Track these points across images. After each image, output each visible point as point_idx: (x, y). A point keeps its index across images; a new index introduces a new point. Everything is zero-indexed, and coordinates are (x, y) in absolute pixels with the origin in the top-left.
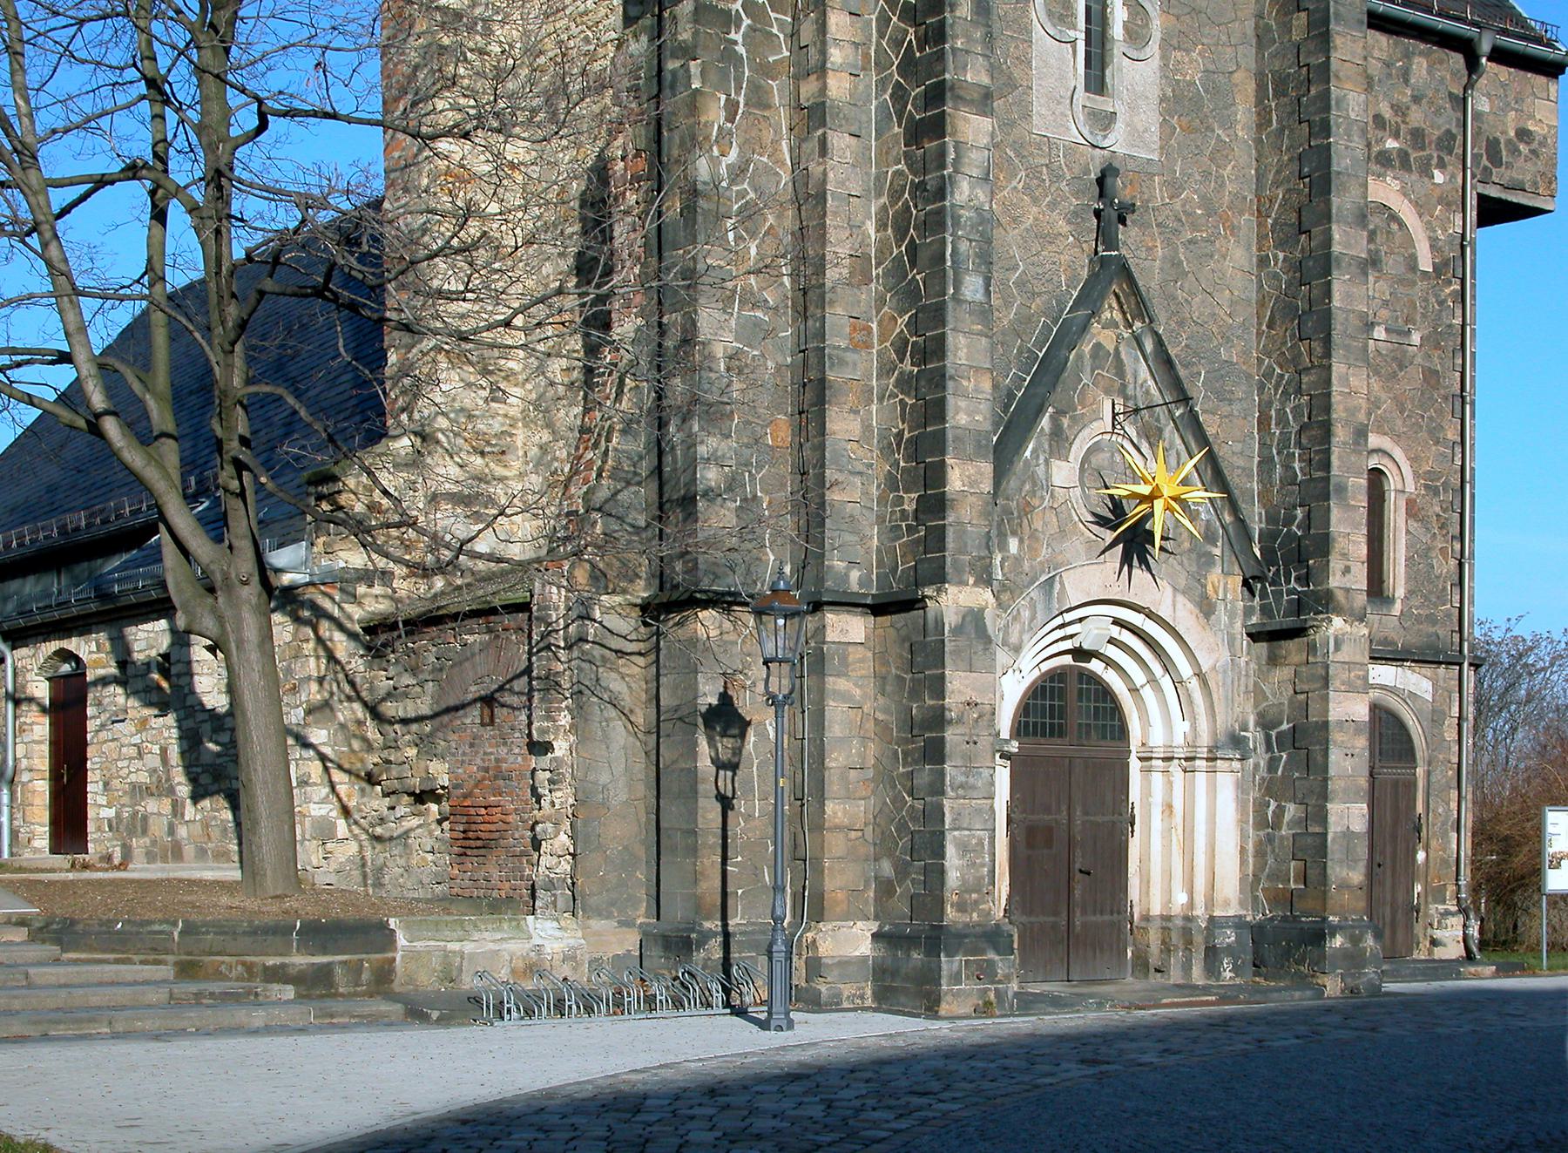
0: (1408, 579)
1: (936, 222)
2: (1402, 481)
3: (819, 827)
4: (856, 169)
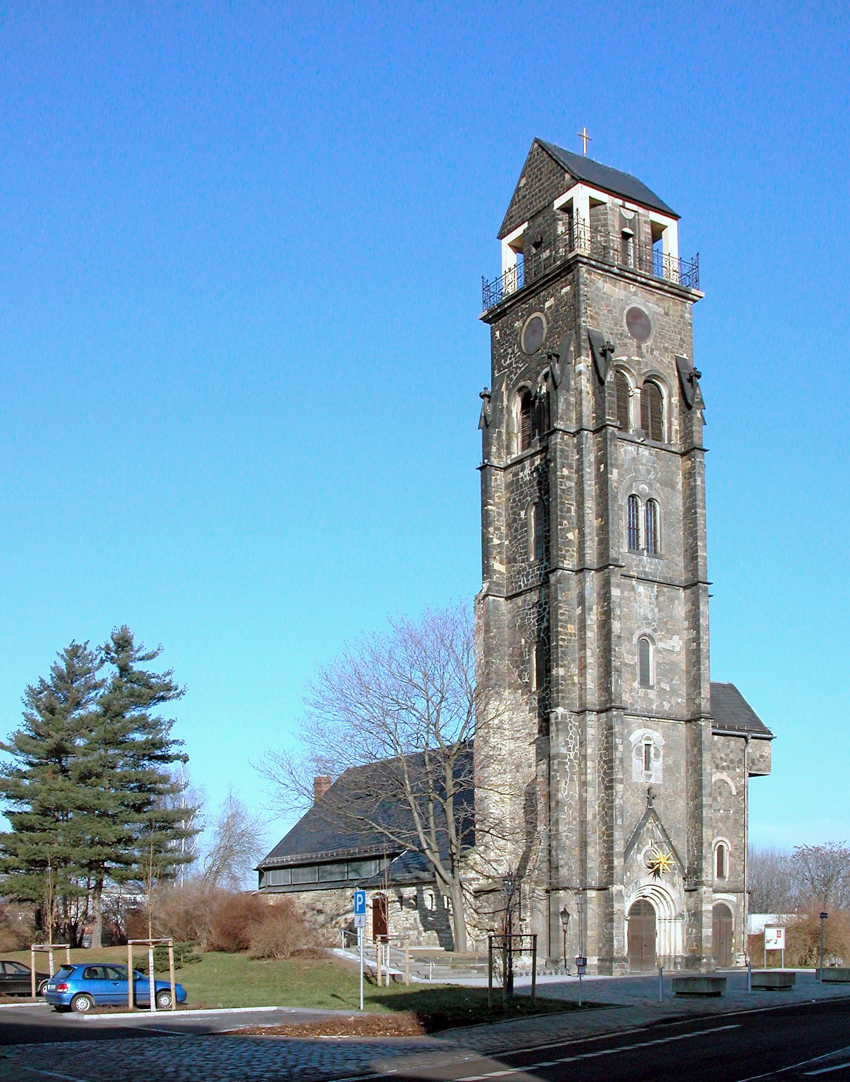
1: (611, 808)
3: (586, 936)
4: (593, 795)
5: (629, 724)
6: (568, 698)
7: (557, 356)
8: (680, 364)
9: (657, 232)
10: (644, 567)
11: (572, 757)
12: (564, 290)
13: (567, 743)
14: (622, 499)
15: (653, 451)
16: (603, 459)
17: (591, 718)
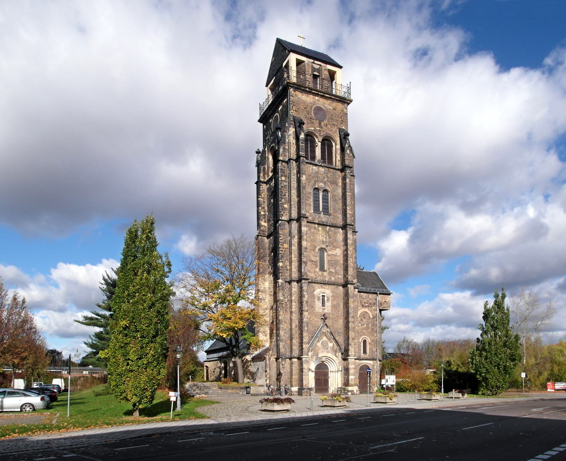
1: (302, 323)
4: (295, 317)
5: (313, 287)
8: (340, 130)
16: (299, 172)
17: (294, 284)
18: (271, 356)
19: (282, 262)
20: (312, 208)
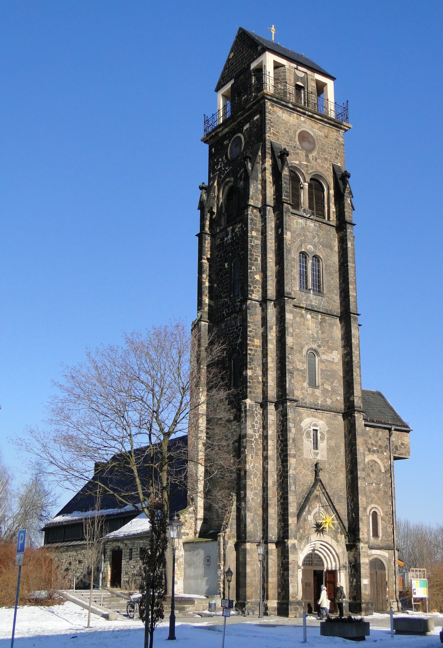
0: (382, 533)
2: (380, 513)
3: (267, 582)
4: (272, 466)
5: (300, 414)
6: (254, 393)
7: (250, 159)
9: (321, 88)
10: (311, 301)
11: (257, 437)
12: (256, 118)
13: (253, 426)
14: (295, 254)
15: (317, 224)
16: (280, 226)
18: (229, 538)
19: (251, 369)
20: (298, 283)
